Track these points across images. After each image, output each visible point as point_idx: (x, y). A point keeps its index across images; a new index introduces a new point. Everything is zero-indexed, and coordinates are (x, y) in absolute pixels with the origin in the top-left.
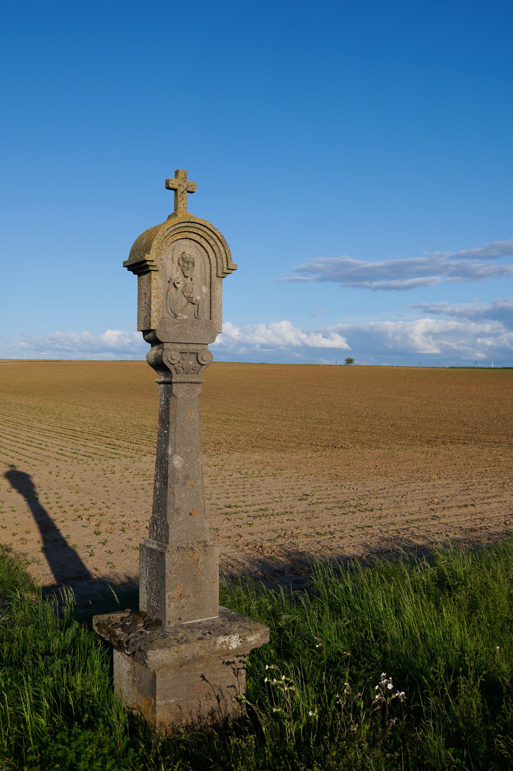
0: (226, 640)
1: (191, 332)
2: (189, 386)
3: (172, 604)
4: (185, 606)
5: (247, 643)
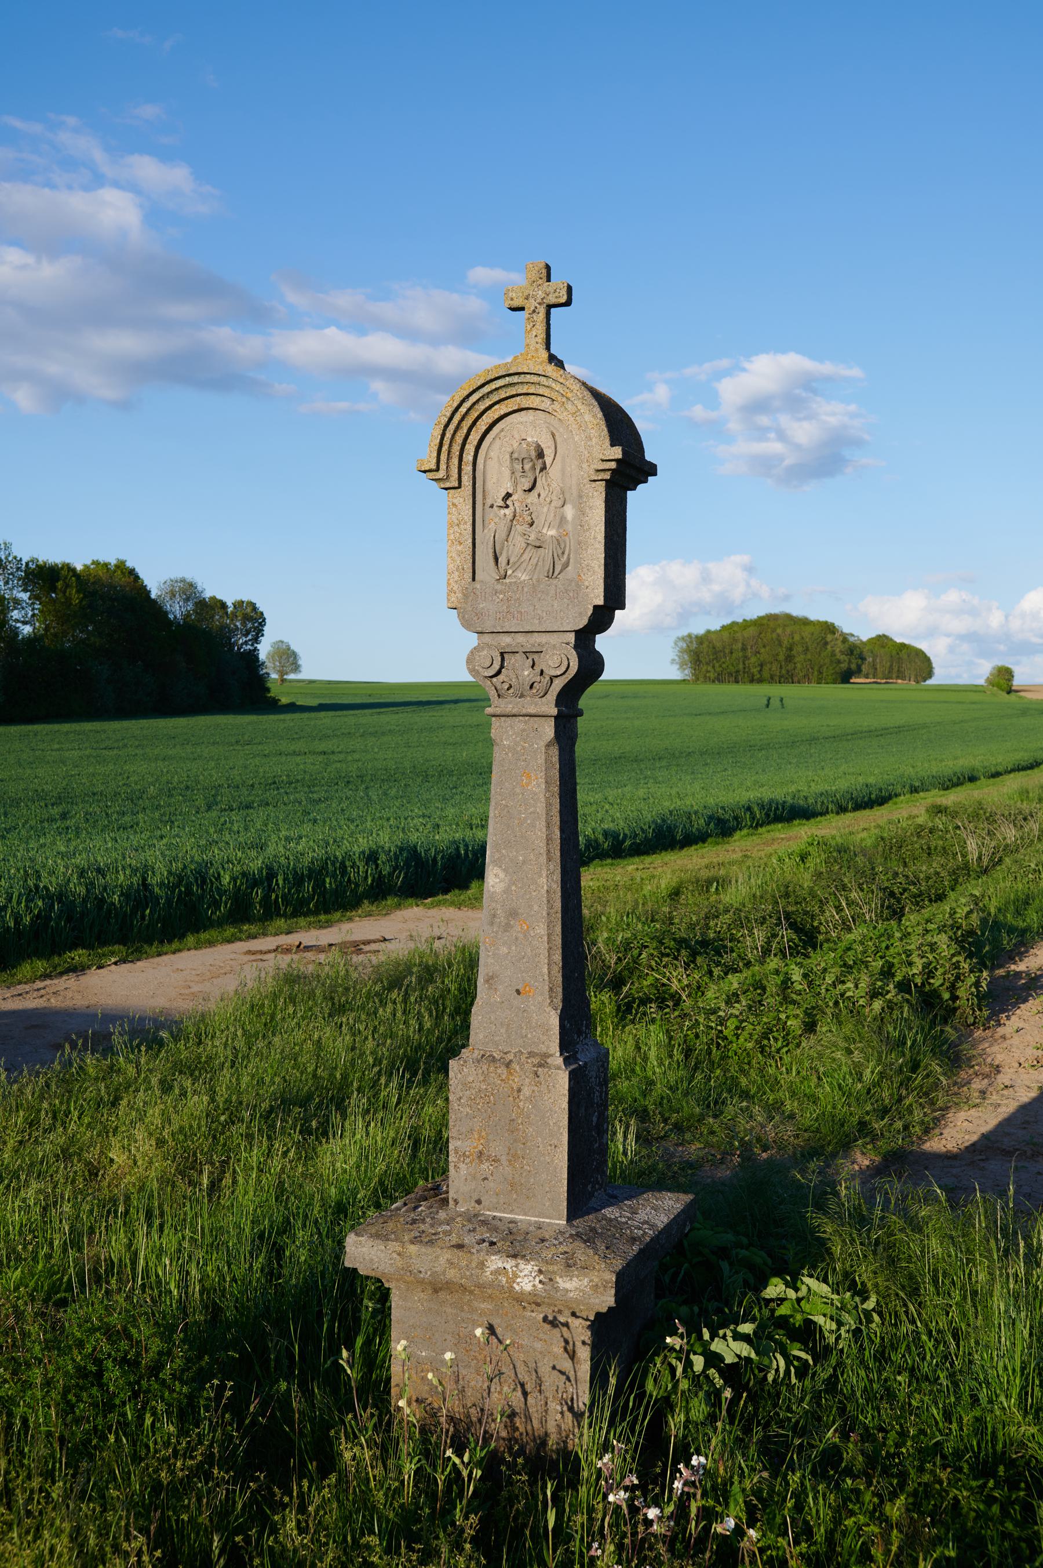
0: (508, 1267)
1: (532, 608)
2: (526, 722)
3: (462, 1166)
4: (491, 1178)
5: (557, 1289)
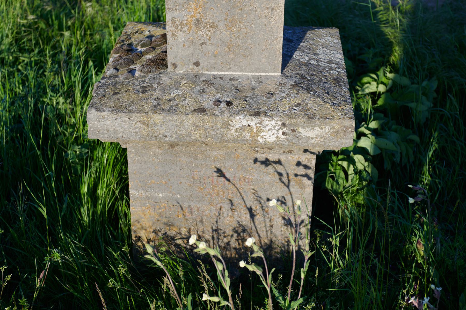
0: (252, 124)
3: (179, 34)
4: (208, 42)
5: (299, 138)
